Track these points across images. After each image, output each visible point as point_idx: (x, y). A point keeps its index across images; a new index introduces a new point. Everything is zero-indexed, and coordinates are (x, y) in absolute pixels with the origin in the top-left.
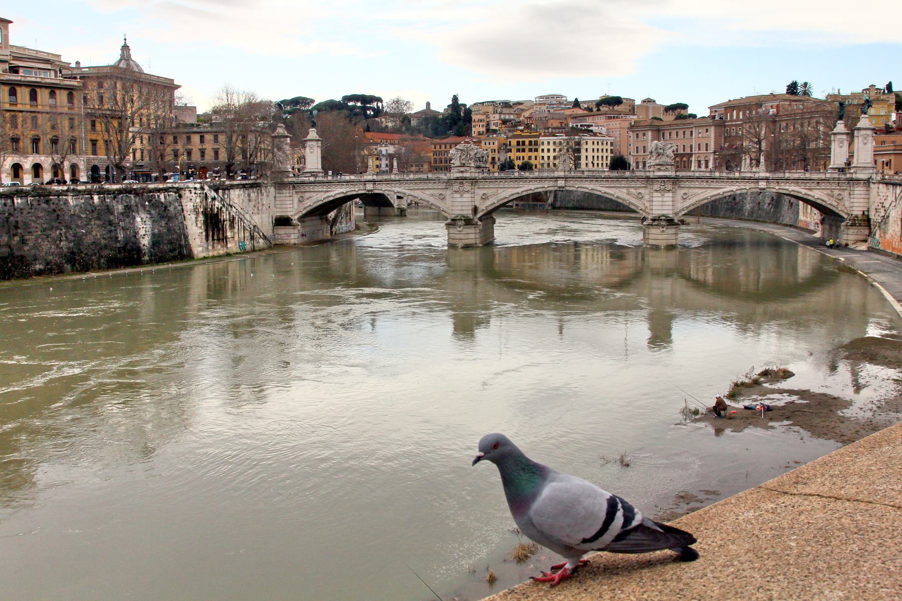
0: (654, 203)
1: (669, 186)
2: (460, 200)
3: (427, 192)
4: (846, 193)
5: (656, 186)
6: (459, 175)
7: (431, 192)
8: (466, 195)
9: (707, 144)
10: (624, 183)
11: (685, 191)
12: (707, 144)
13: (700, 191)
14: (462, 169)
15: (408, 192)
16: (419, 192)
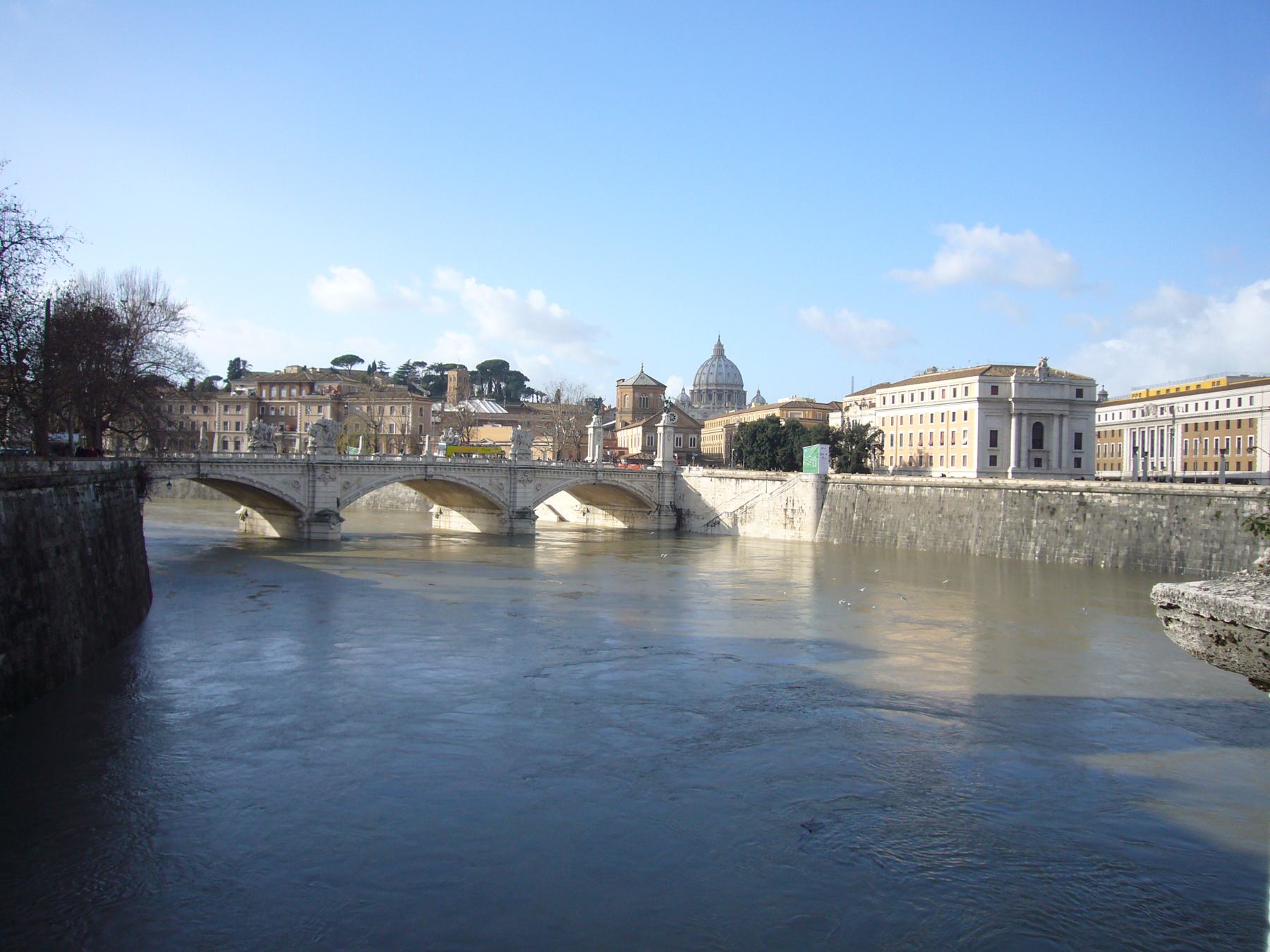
0: (518, 495)
1: (530, 476)
2: (324, 489)
3: (279, 478)
4: (655, 486)
5: (519, 476)
6: (323, 458)
7: (284, 477)
8: (331, 483)
9: (238, 424)
10: (487, 473)
11: (538, 482)
12: (238, 424)
13: (550, 482)
14: (326, 450)
15: (255, 479)
16: (267, 477)
